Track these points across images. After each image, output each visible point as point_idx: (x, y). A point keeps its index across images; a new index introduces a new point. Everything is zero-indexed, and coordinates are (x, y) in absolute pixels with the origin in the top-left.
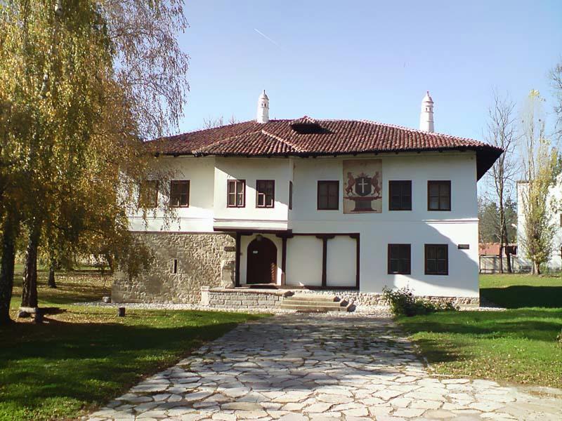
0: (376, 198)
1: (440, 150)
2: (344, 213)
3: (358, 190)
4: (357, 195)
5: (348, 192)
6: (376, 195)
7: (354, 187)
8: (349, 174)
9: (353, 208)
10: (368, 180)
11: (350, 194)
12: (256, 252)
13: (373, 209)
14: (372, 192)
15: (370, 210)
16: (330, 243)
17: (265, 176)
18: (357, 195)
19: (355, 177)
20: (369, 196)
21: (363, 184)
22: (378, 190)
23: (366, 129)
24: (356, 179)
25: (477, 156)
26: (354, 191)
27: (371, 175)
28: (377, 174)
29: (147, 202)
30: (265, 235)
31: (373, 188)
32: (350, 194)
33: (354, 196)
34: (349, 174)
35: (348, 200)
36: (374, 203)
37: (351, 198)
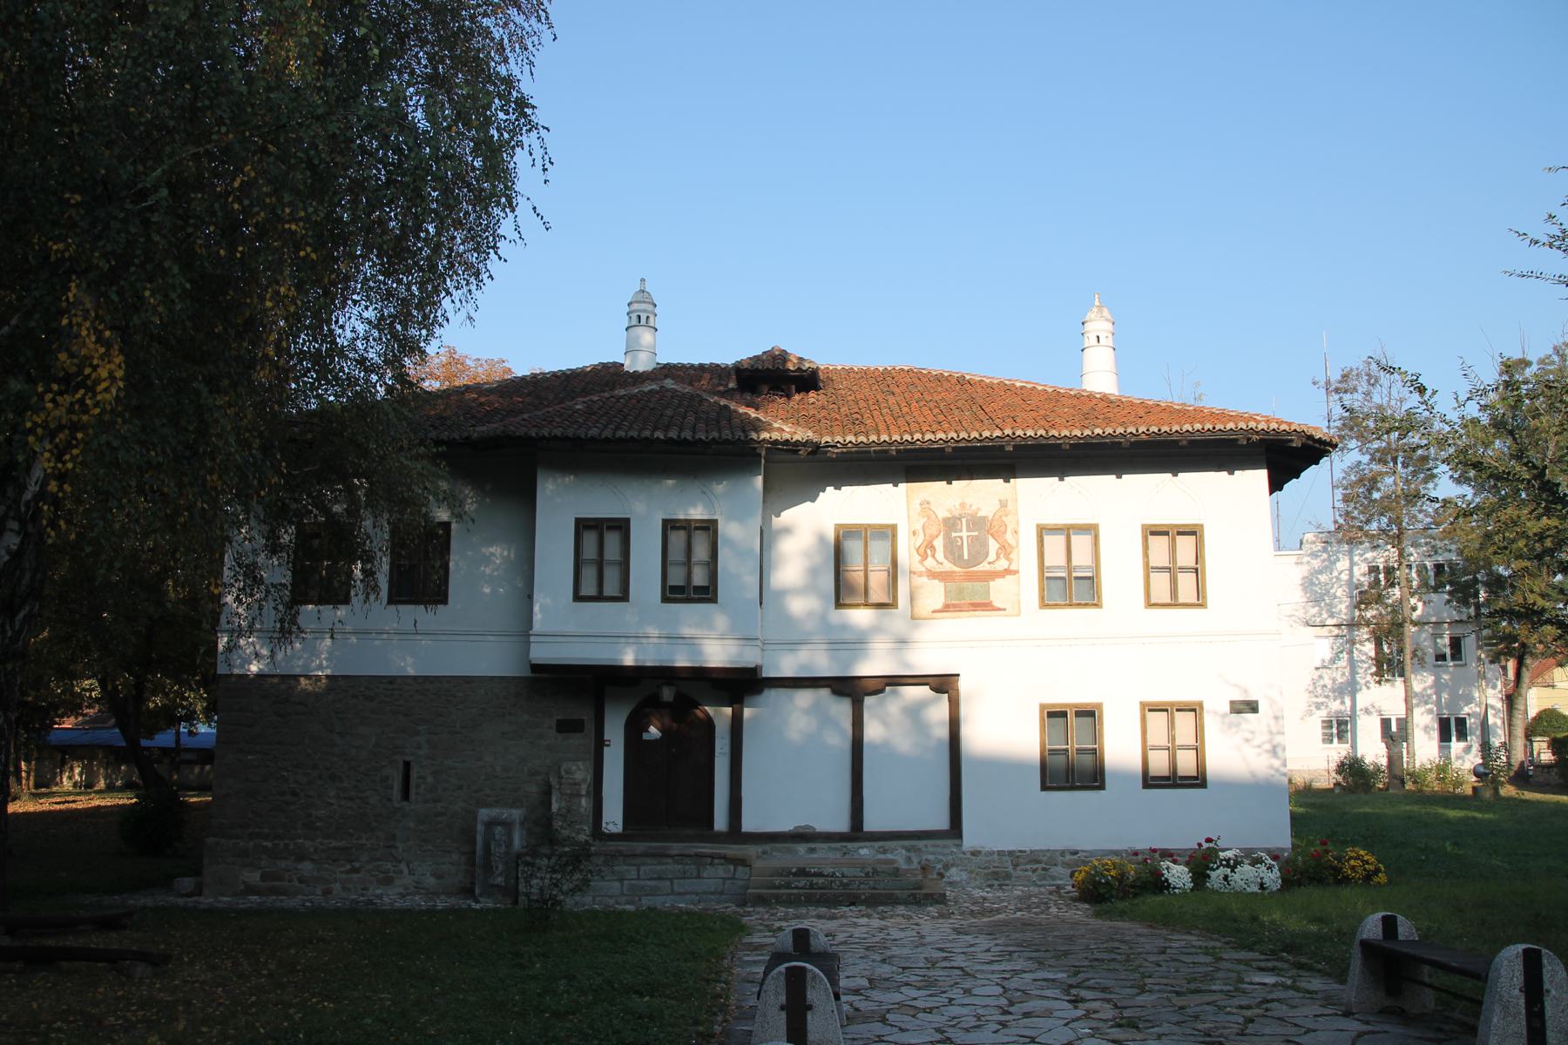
0: (1008, 572)
3: (953, 550)
4: (948, 566)
5: (924, 557)
6: (1002, 564)
7: (939, 543)
10: (977, 523)
11: (930, 563)
13: (996, 604)
14: (992, 556)
15: (986, 606)
18: (948, 566)
20: (984, 567)
21: (964, 534)
22: (1005, 550)
24: (946, 520)
26: (940, 555)
27: (987, 510)
28: (1003, 504)
29: (319, 577)
31: (993, 546)
32: (930, 563)
33: (939, 569)
35: (925, 579)
36: (999, 591)
37: (933, 575)
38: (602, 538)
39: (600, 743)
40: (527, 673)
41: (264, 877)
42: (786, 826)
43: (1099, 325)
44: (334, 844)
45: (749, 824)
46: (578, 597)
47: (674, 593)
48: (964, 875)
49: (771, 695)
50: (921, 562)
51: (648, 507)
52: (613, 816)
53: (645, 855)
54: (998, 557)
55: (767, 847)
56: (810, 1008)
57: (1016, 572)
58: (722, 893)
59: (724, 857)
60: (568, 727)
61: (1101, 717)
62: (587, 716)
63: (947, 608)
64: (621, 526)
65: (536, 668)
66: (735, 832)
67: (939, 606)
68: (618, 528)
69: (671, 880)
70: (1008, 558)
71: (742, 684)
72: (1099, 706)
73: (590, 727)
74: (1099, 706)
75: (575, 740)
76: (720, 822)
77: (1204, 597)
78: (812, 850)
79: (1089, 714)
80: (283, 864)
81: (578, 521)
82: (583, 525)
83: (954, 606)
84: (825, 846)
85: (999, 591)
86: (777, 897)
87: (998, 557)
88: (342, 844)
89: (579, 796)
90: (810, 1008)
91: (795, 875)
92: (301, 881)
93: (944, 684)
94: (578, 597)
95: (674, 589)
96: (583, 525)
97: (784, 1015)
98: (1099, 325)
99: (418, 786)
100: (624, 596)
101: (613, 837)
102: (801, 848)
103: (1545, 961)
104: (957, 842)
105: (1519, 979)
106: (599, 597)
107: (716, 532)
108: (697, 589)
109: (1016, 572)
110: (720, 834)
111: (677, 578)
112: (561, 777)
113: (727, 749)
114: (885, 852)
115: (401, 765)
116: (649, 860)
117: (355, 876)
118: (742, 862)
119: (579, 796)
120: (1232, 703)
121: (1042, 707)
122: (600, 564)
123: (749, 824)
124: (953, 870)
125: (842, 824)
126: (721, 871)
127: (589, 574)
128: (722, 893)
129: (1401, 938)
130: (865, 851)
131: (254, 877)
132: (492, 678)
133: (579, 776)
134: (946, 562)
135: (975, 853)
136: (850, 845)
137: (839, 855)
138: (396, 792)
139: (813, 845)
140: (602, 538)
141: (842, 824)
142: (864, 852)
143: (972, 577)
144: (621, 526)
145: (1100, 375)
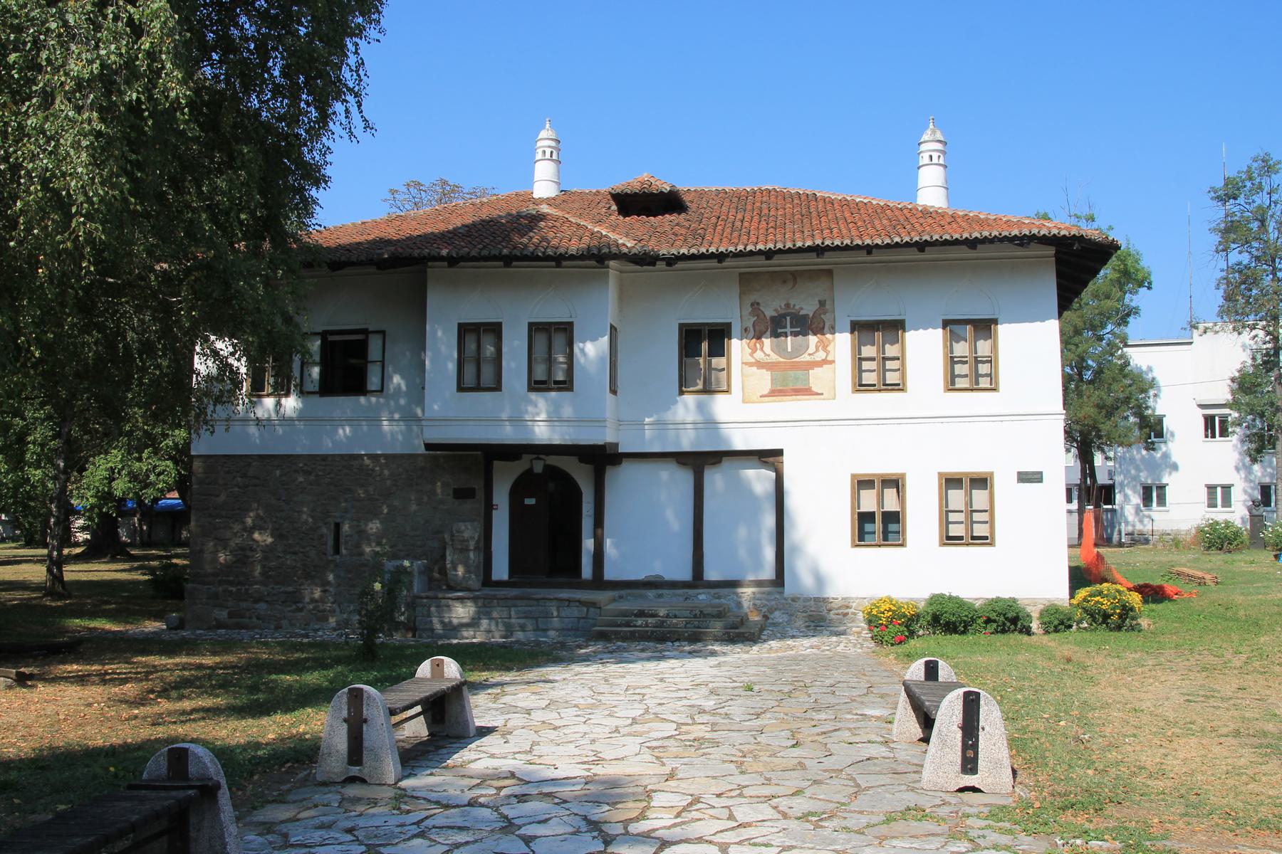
0: (825, 362)
1: (972, 243)
2: (744, 402)
4: (774, 357)
6: (821, 355)
8: (755, 305)
9: (766, 387)
12: (530, 501)
13: (815, 389)
14: (812, 349)
15: (807, 391)
16: (715, 479)
17: (553, 312)
18: (774, 357)
19: (769, 313)
20: (805, 358)
23: (808, 205)
24: (773, 318)
25: (1059, 262)
30: (553, 460)
34: (755, 305)
35: (754, 369)
36: (817, 378)
37: (760, 365)
38: (478, 337)
39: (489, 507)
40: (422, 450)
41: (231, 615)
42: (641, 576)
43: (930, 147)
44: (283, 589)
45: (610, 574)
46: (461, 388)
47: (537, 386)
48: (786, 618)
49: (627, 468)
50: (751, 355)
51: (516, 313)
52: (501, 570)
53: (516, 598)
54: (817, 350)
55: (623, 592)
56: (366, 721)
57: (832, 362)
58: (577, 630)
59: (579, 601)
60: (463, 494)
61: (903, 486)
62: (478, 485)
63: (774, 393)
64: (495, 329)
65: (428, 446)
66: (599, 582)
67: (766, 392)
68: (494, 331)
69: (536, 619)
70: (825, 349)
71: (602, 458)
72: (903, 476)
73: (480, 494)
74: (903, 476)
75: (468, 505)
76: (587, 571)
77: (997, 383)
78: (660, 596)
79: (895, 482)
80: (244, 605)
81: (461, 326)
82: (465, 330)
83: (780, 391)
84: (671, 592)
85: (817, 378)
86: (616, 633)
87: (817, 350)
88: (290, 589)
89: (468, 550)
90: (366, 721)
91: (636, 615)
92: (258, 618)
93: (769, 457)
94: (461, 388)
95: (537, 382)
96: (465, 330)
97: (345, 726)
98: (930, 147)
99: (346, 543)
100: (497, 387)
101: (500, 584)
102: (651, 593)
103: (982, 702)
104: (779, 589)
105: (958, 717)
106: (478, 388)
107: (572, 332)
108: (556, 382)
109: (832, 362)
110: (587, 581)
111: (540, 374)
112: (453, 535)
113: (592, 512)
114: (719, 598)
115: (332, 527)
116: (519, 602)
117: (299, 615)
118: (593, 604)
119: (468, 550)
120: (1019, 473)
121: (853, 476)
122: (478, 362)
123: (610, 574)
124: (777, 613)
125: (685, 574)
126: (575, 612)
127: (470, 371)
128: (577, 630)
129: (940, 679)
130: (703, 596)
131: (223, 614)
132: (402, 456)
133: (466, 535)
134: (772, 354)
135: (793, 600)
136: (691, 592)
137: (681, 599)
138: (330, 549)
139: (660, 592)
140: (478, 337)
141: (685, 574)
142: (701, 597)
143: (796, 366)
144: (495, 329)
145: (931, 191)
